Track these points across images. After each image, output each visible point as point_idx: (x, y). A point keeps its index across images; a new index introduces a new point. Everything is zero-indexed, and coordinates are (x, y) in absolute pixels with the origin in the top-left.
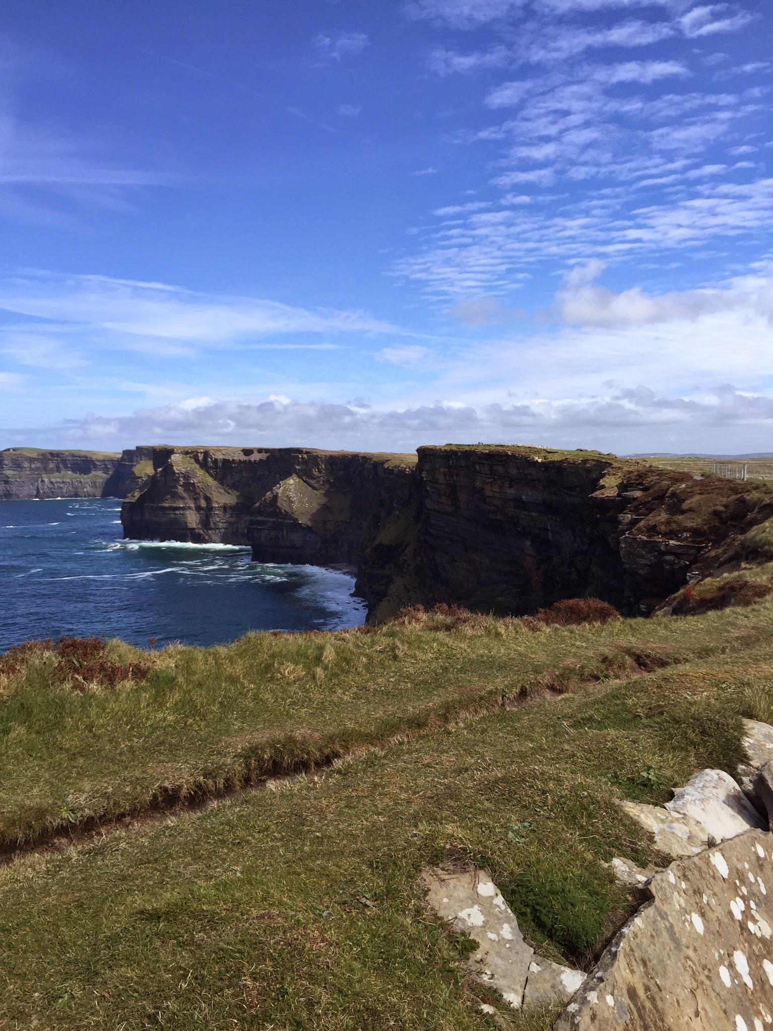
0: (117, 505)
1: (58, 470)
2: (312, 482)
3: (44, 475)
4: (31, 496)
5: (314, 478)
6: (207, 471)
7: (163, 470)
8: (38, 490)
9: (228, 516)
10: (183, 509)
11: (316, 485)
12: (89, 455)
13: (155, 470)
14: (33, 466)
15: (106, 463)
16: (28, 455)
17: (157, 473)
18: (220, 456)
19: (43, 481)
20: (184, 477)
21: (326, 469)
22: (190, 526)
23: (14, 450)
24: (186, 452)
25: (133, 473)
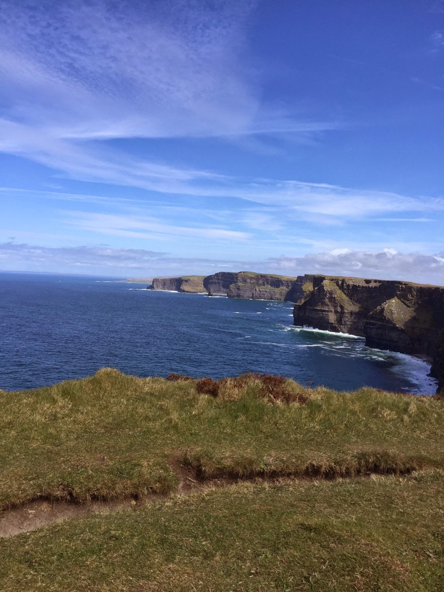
0: (292, 306)
1: (264, 285)
2: (407, 302)
3: (256, 287)
4: (249, 297)
5: (408, 300)
6: (343, 291)
7: (318, 289)
8: (253, 294)
9: (353, 318)
10: (328, 311)
11: (409, 304)
13: (314, 288)
15: (288, 283)
16: (250, 275)
17: (314, 290)
18: (351, 283)
19: (256, 290)
21: (417, 295)
22: (330, 321)
23: (244, 272)
24: (332, 279)
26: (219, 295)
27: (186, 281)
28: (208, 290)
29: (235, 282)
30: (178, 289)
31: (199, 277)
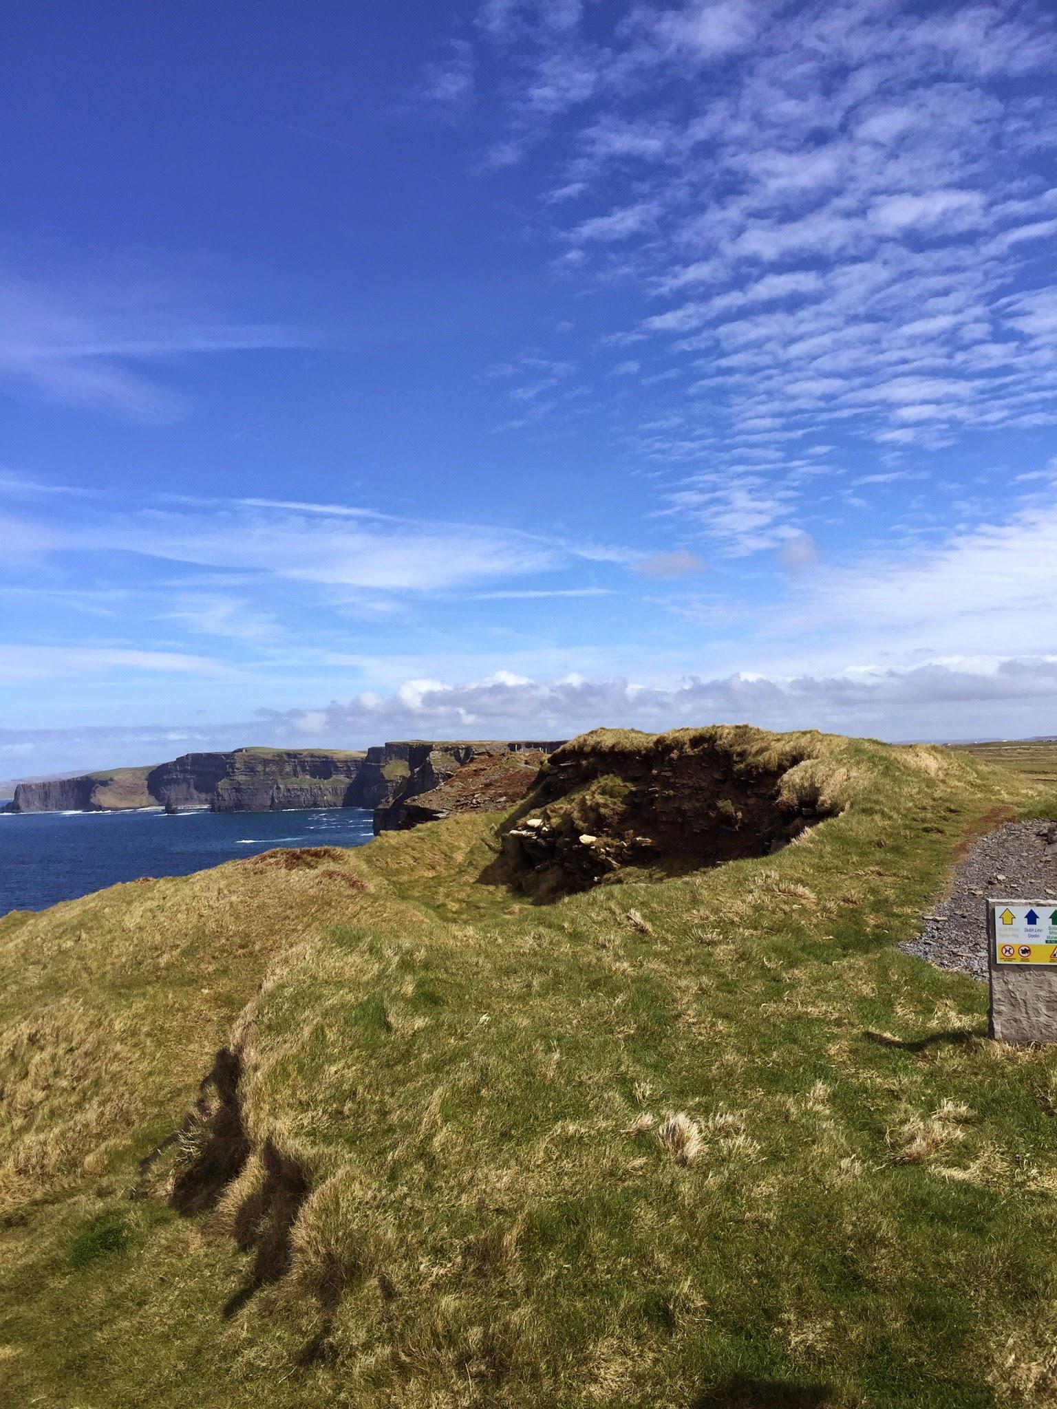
0: (367, 815)
1: (296, 775)
3: (279, 781)
8: (273, 799)
13: (412, 770)
19: (278, 788)
25: (382, 776)
26: (194, 808)
27: (104, 783)
28: (160, 799)
29: (228, 774)
30: (85, 803)
31: (134, 771)
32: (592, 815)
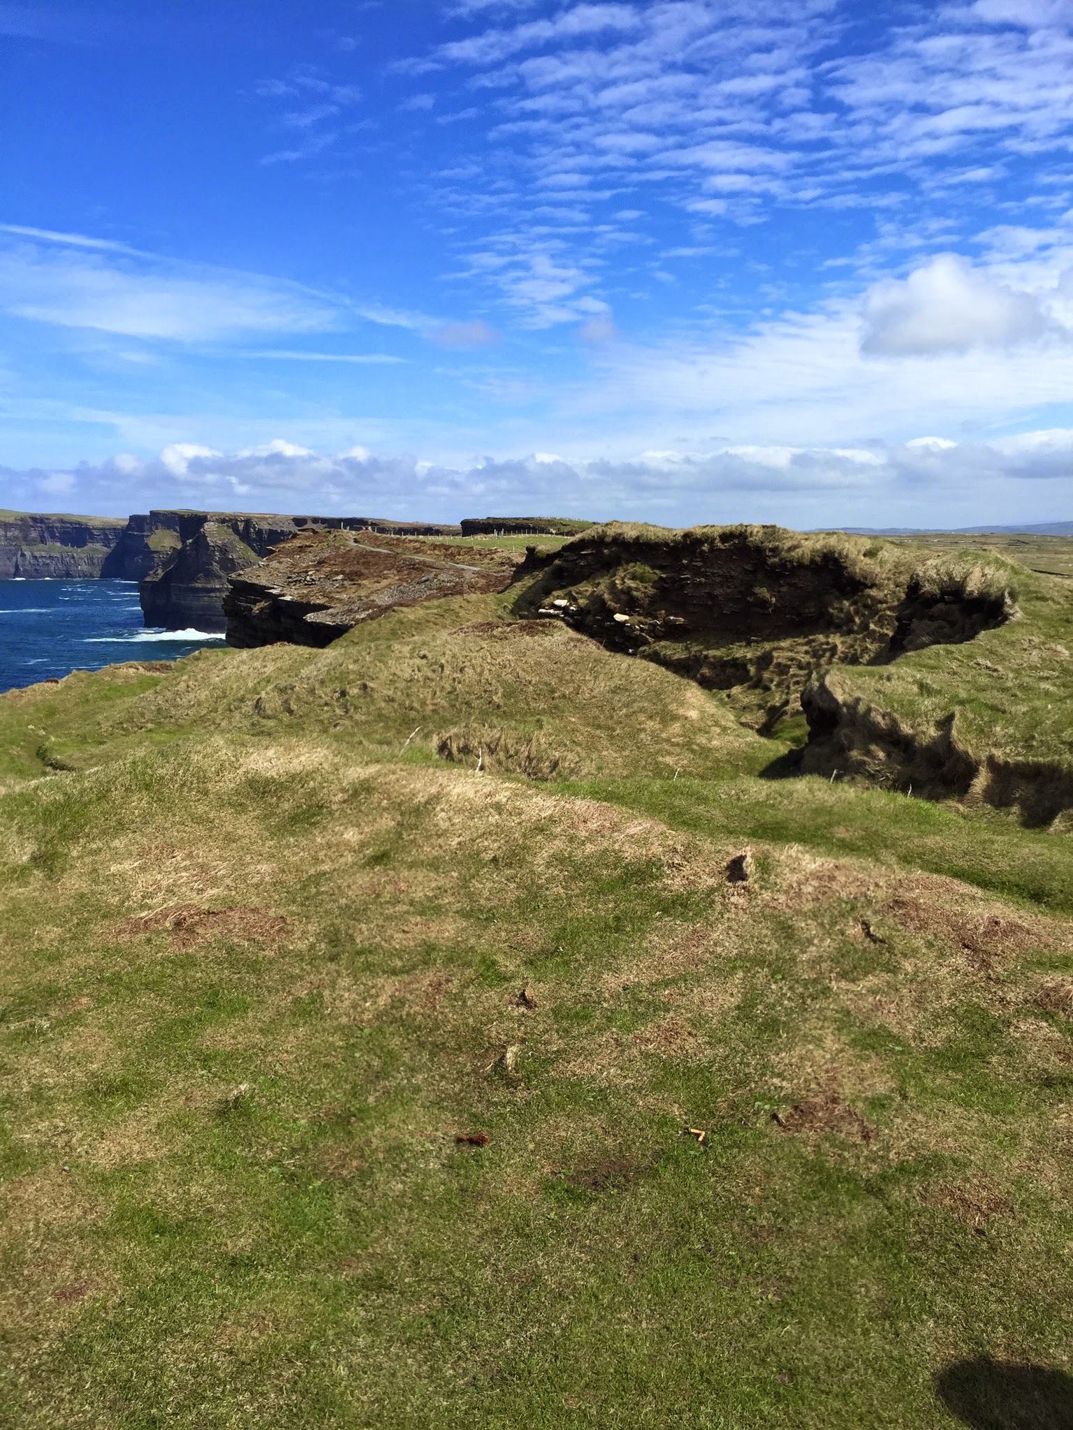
0: (131, 588)
1: (43, 541)
4: (8, 575)
6: (250, 545)
12: (84, 521)
13: (184, 542)
14: (9, 534)
15: (106, 533)
19: (23, 555)
20: (220, 551)
32: (623, 597)
